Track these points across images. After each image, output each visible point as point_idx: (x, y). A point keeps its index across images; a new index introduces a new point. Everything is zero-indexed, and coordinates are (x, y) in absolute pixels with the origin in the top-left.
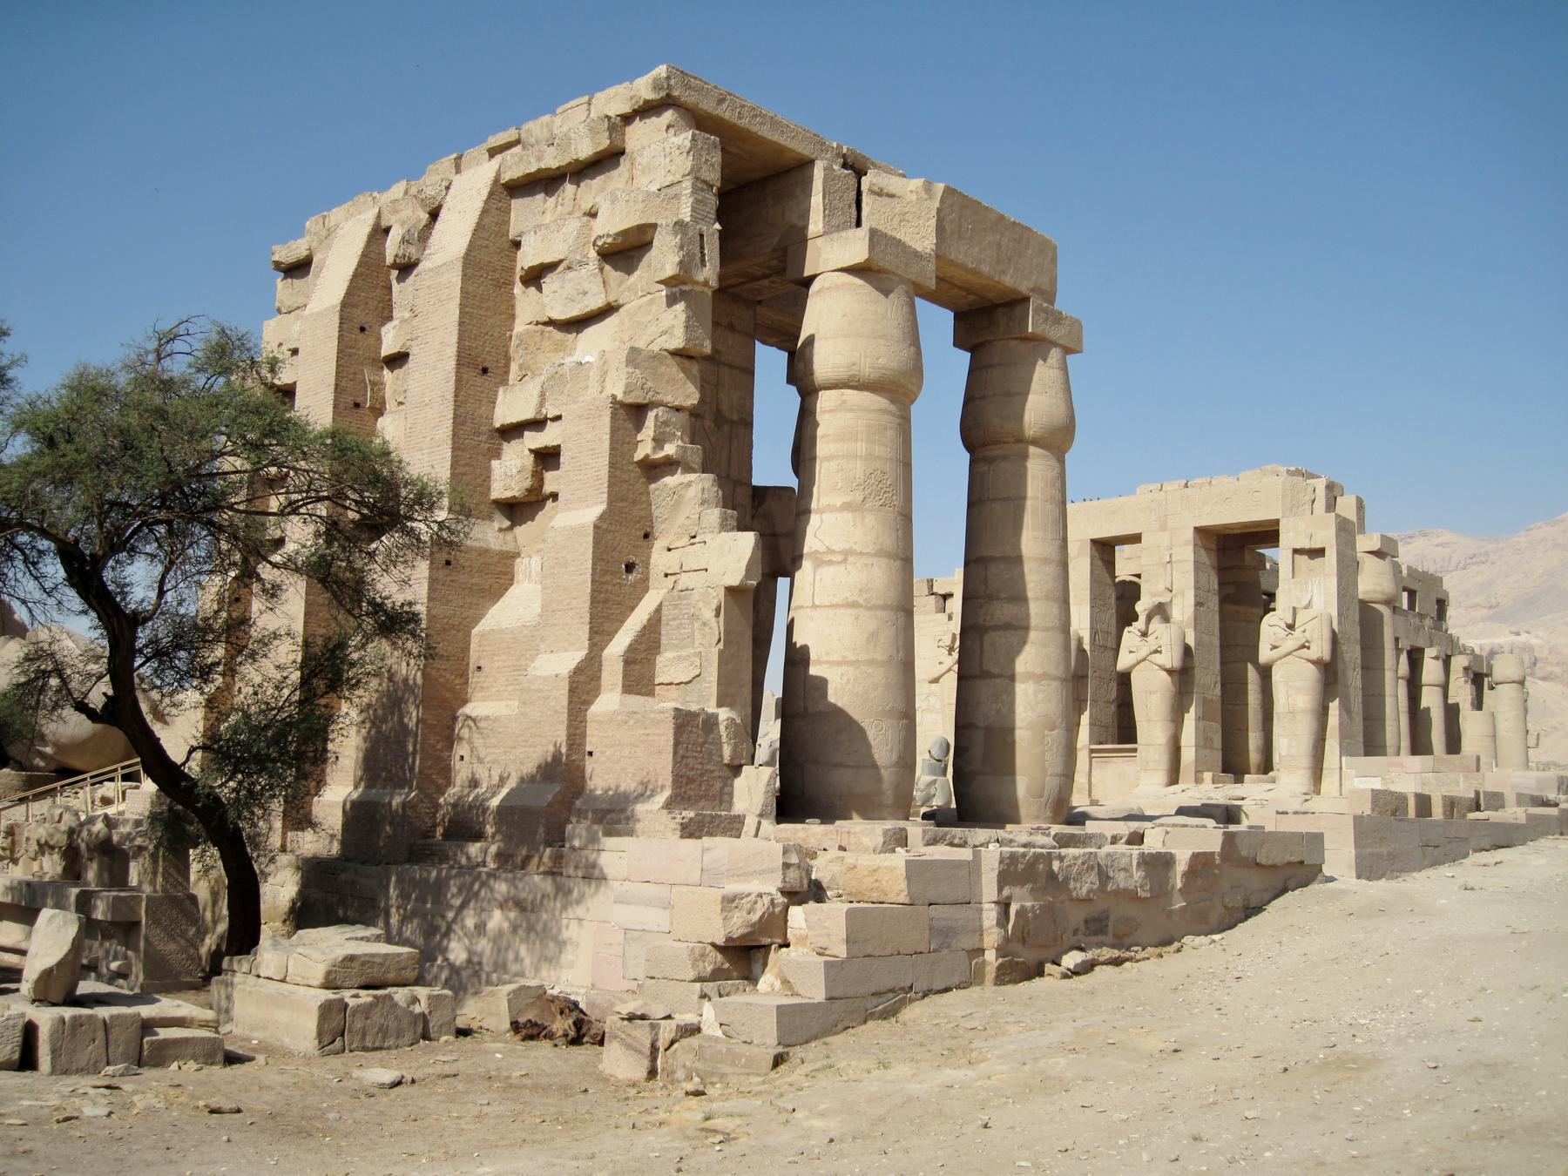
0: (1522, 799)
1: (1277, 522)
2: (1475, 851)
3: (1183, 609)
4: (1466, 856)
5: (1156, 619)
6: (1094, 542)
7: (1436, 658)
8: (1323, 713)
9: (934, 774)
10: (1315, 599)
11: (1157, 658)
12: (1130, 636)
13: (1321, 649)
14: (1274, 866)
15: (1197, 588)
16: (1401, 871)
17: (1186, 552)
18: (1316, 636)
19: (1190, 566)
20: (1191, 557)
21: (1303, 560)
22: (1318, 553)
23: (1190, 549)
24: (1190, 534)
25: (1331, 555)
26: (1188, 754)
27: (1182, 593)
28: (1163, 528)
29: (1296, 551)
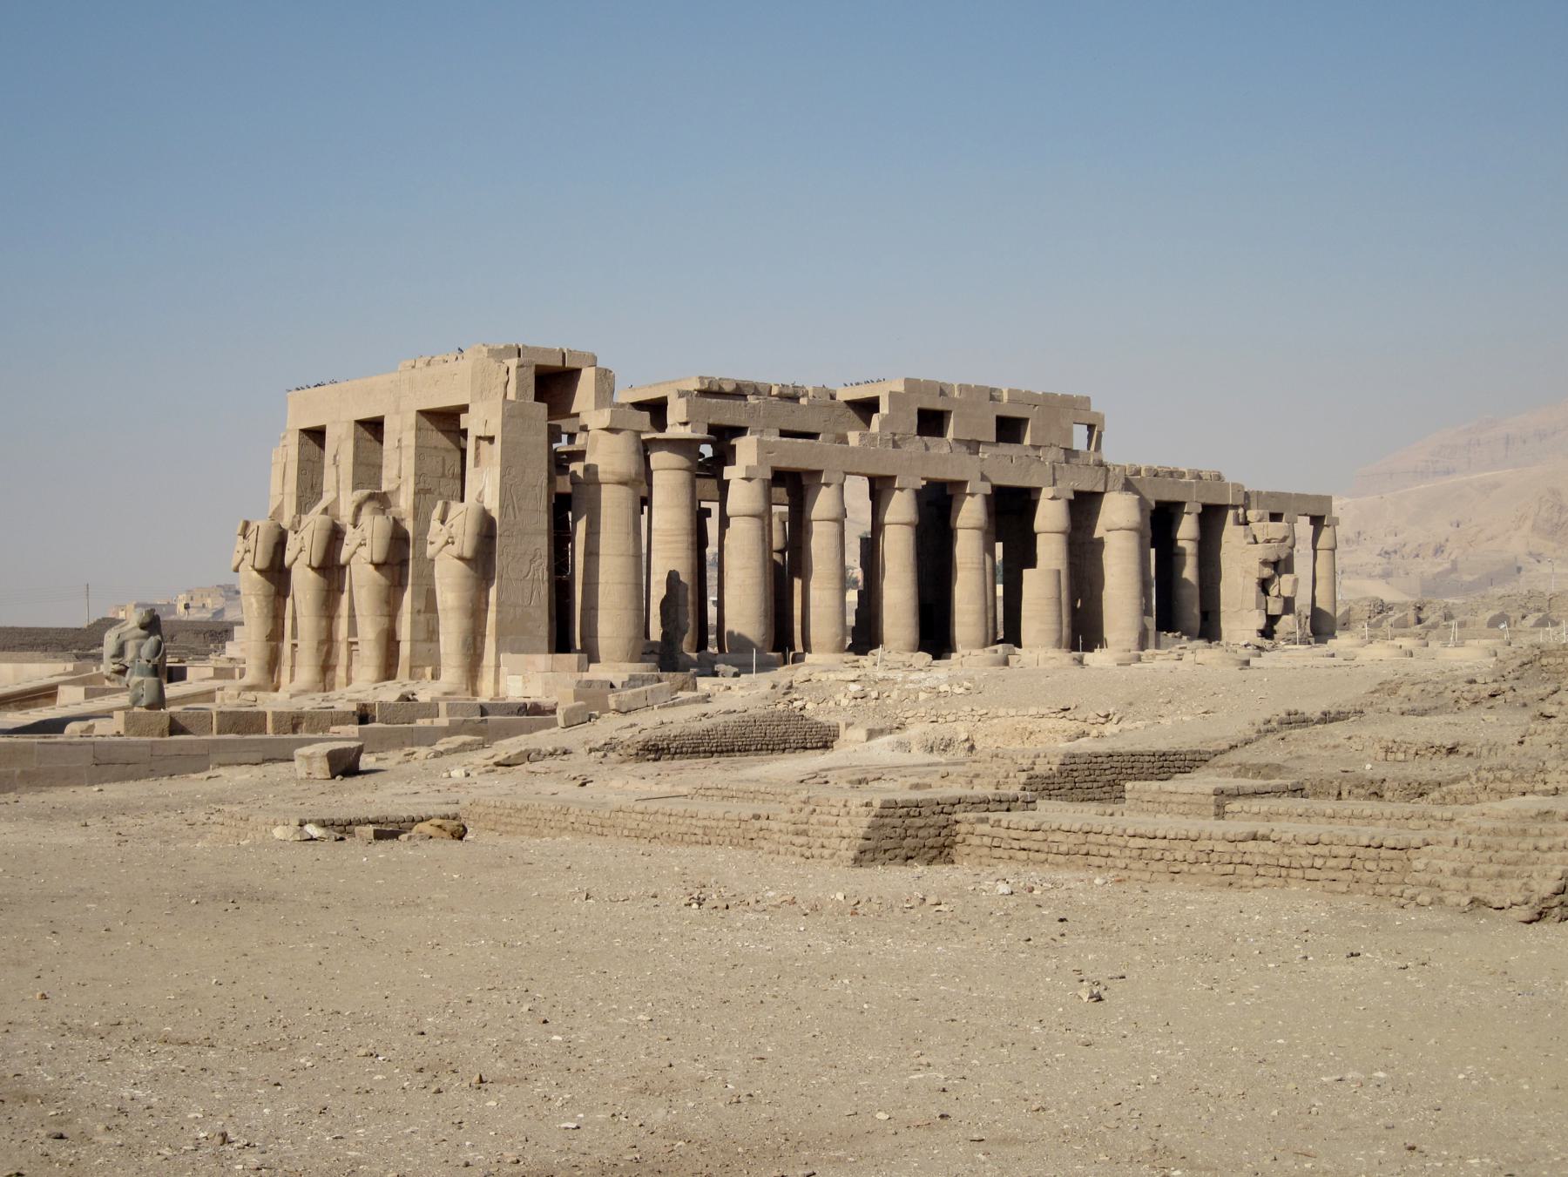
2: (220, 765)
4: (207, 769)
5: (366, 510)
7: (1053, 498)
8: (476, 613)
9: (141, 674)
13: (466, 545)
15: (419, 475)
16: (51, 785)
18: (461, 531)
19: (412, 452)
20: (412, 442)
21: (484, 444)
22: (491, 439)
24: (411, 418)
25: (498, 441)
26: (405, 649)
28: (397, 412)
29: (479, 438)
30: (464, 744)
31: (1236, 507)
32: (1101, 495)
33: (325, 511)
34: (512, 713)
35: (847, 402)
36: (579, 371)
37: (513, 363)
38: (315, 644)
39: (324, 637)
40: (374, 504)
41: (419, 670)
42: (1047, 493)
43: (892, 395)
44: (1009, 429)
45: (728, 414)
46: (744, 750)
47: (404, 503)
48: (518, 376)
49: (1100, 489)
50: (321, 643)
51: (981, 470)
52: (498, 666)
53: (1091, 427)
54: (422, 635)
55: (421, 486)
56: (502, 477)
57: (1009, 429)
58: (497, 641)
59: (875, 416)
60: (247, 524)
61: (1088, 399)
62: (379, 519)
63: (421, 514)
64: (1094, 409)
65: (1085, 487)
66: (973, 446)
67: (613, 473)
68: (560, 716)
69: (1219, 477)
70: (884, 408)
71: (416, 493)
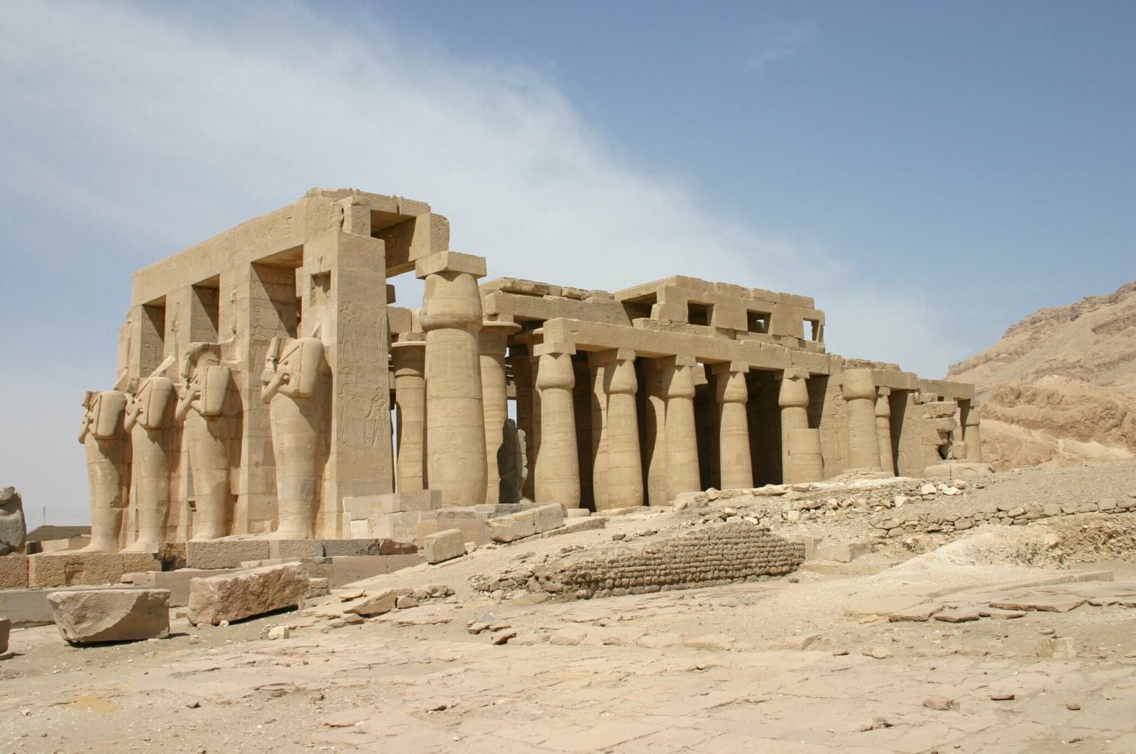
23: (247, 285)
24: (247, 269)
26: (242, 505)
27: (242, 332)
31: (913, 391)
32: (827, 376)
34: (362, 552)
35: (624, 302)
36: (413, 219)
37: (347, 203)
38: (154, 506)
39: (163, 497)
40: (210, 356)
41: (257, 525)
42: (788, 374)
43: (667, 288)
44: (756, 321)
45: (531, 309)
46: (699, 580)
47: (238, 356)
48: (353, 215)
49: (825, 372)
50: (160, 504)
51: (745, 354)
52: (340, 512)
53: (815, 323)
54: (261, 489)
55: (256, 337)
56: (340, 311)
57: (756, 321)
58: (340, 484)
59: (654, 306)
60: (90, 395)
61: (812, 301)
62: (213, 369)
63: (254, 363)
64: (817, 307)
65: (816, 370)
66: (733, 333)
67: (452, 315)
68: (428, 553)
69: (897, 368)
71: (252, 345)
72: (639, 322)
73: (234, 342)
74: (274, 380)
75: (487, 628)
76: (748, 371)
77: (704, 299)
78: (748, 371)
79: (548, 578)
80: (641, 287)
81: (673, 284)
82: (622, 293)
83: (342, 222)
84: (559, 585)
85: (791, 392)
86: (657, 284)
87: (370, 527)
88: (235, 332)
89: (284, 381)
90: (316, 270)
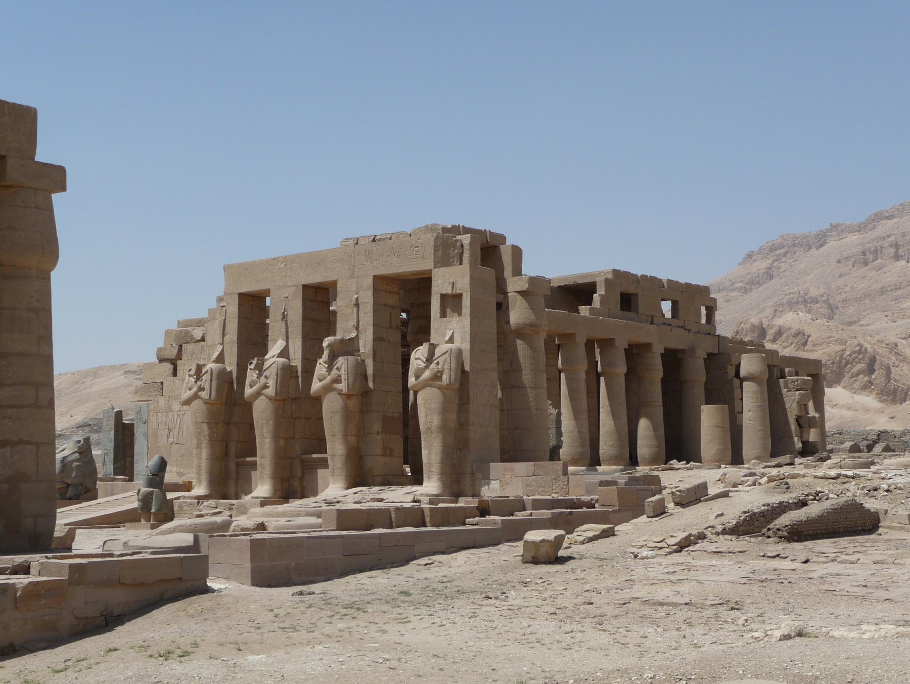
0: (538, 505)
1: (431, 270)
3: (366, 345)
6: (306, 287)
10: (455, 335)
11: (338, 386)
12: (321, 368)
14: (142, 584)
17: (367, 298)
18: (447, 366)
24: (369, 281)
28: (352, 276)
30: (604, 531)
33: (280, 355)
35: (560, 287)
37: (466, 239)
43: (606, 280)
70: (601, 291)
72: (584, 310)
73: (357, 336)
74: (427, 374)
75: (778, 555)
76: (663, 352)
77: (631, 290)
78: (663, 352)
79: (778, 530)
80: (579, 276)
81: (610, 276)
82: (559, 279)
83: (462, 254)
84: (785, 534)
85: (696, 373)
86: (599, 274)
87: (501, 486)
88: (357, 328)
89: (437, 376)
90: (448, 290)
